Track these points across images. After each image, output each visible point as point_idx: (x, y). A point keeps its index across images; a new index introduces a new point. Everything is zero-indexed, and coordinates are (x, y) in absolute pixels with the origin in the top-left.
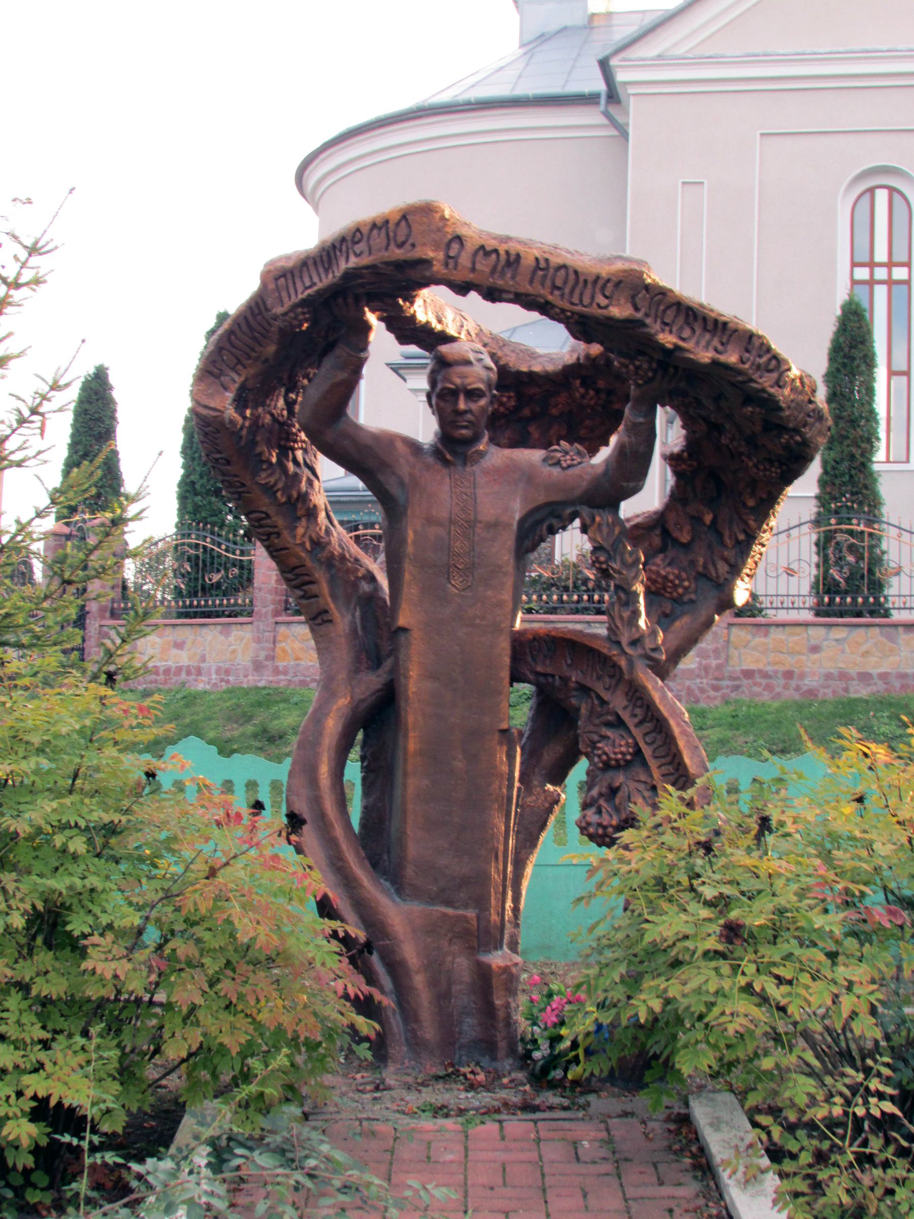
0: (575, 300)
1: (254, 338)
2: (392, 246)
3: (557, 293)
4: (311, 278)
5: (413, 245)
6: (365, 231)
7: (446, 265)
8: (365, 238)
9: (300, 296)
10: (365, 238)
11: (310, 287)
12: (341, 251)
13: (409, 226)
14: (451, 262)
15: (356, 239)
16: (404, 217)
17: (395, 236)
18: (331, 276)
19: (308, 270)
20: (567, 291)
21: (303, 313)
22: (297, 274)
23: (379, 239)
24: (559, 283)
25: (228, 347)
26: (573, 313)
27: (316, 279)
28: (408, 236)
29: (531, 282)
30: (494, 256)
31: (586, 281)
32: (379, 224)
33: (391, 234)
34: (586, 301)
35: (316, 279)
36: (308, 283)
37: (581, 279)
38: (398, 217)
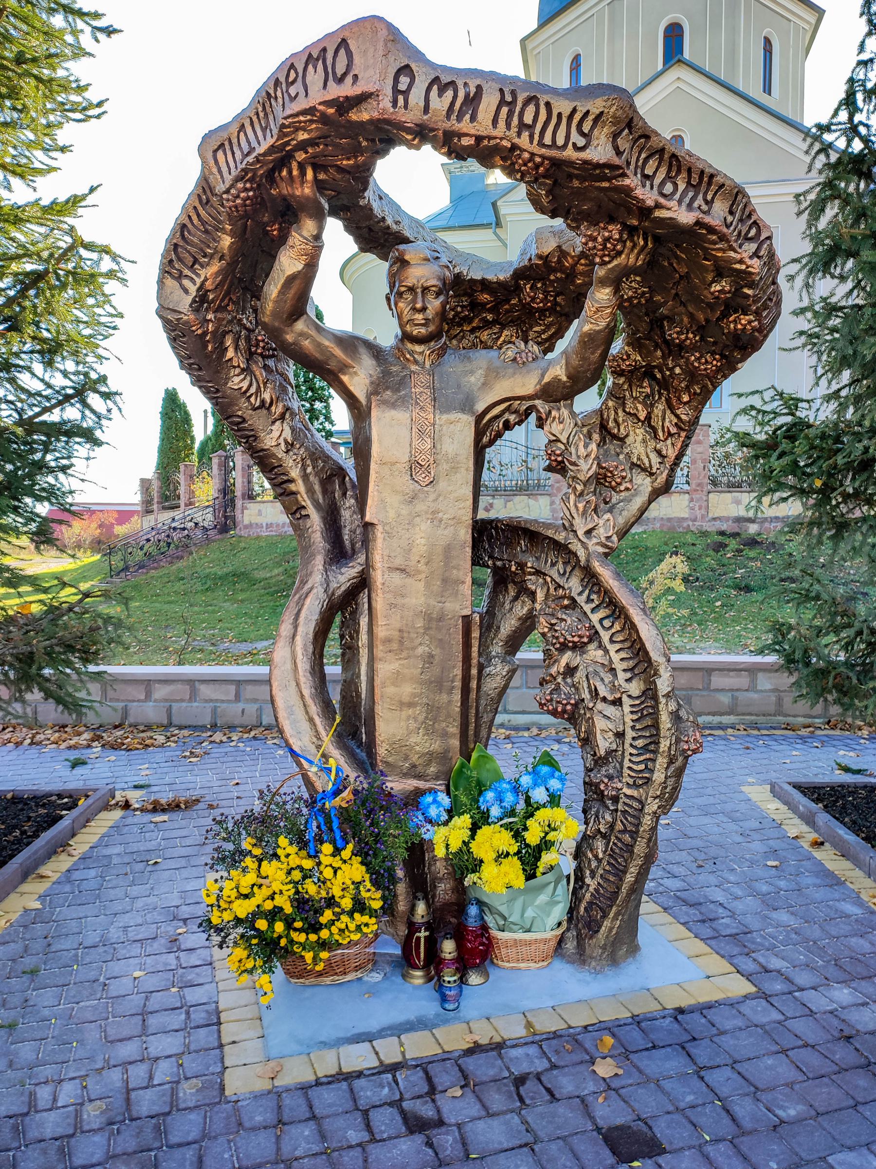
0: (548, 140)
1: (206, 232)
2: (331, 83)
7: (395, 103)
9: (240, 167)
10: (300, 75)
12: (276, 98)
13: (349, 55)
14: (401, 99)
15: (291, 80)
16: (344, 41)
19: (246, 134)
21: (246, 190)
22: (235, 141)
23: (315, 77)
25: (181, 243)
26: (543, 157)
28: (349, 67)
29: (495, 122)
30: (449, 93)
31: (560, 115)
34: (560, 141)
35: (254, 144)
36: (246, 150)
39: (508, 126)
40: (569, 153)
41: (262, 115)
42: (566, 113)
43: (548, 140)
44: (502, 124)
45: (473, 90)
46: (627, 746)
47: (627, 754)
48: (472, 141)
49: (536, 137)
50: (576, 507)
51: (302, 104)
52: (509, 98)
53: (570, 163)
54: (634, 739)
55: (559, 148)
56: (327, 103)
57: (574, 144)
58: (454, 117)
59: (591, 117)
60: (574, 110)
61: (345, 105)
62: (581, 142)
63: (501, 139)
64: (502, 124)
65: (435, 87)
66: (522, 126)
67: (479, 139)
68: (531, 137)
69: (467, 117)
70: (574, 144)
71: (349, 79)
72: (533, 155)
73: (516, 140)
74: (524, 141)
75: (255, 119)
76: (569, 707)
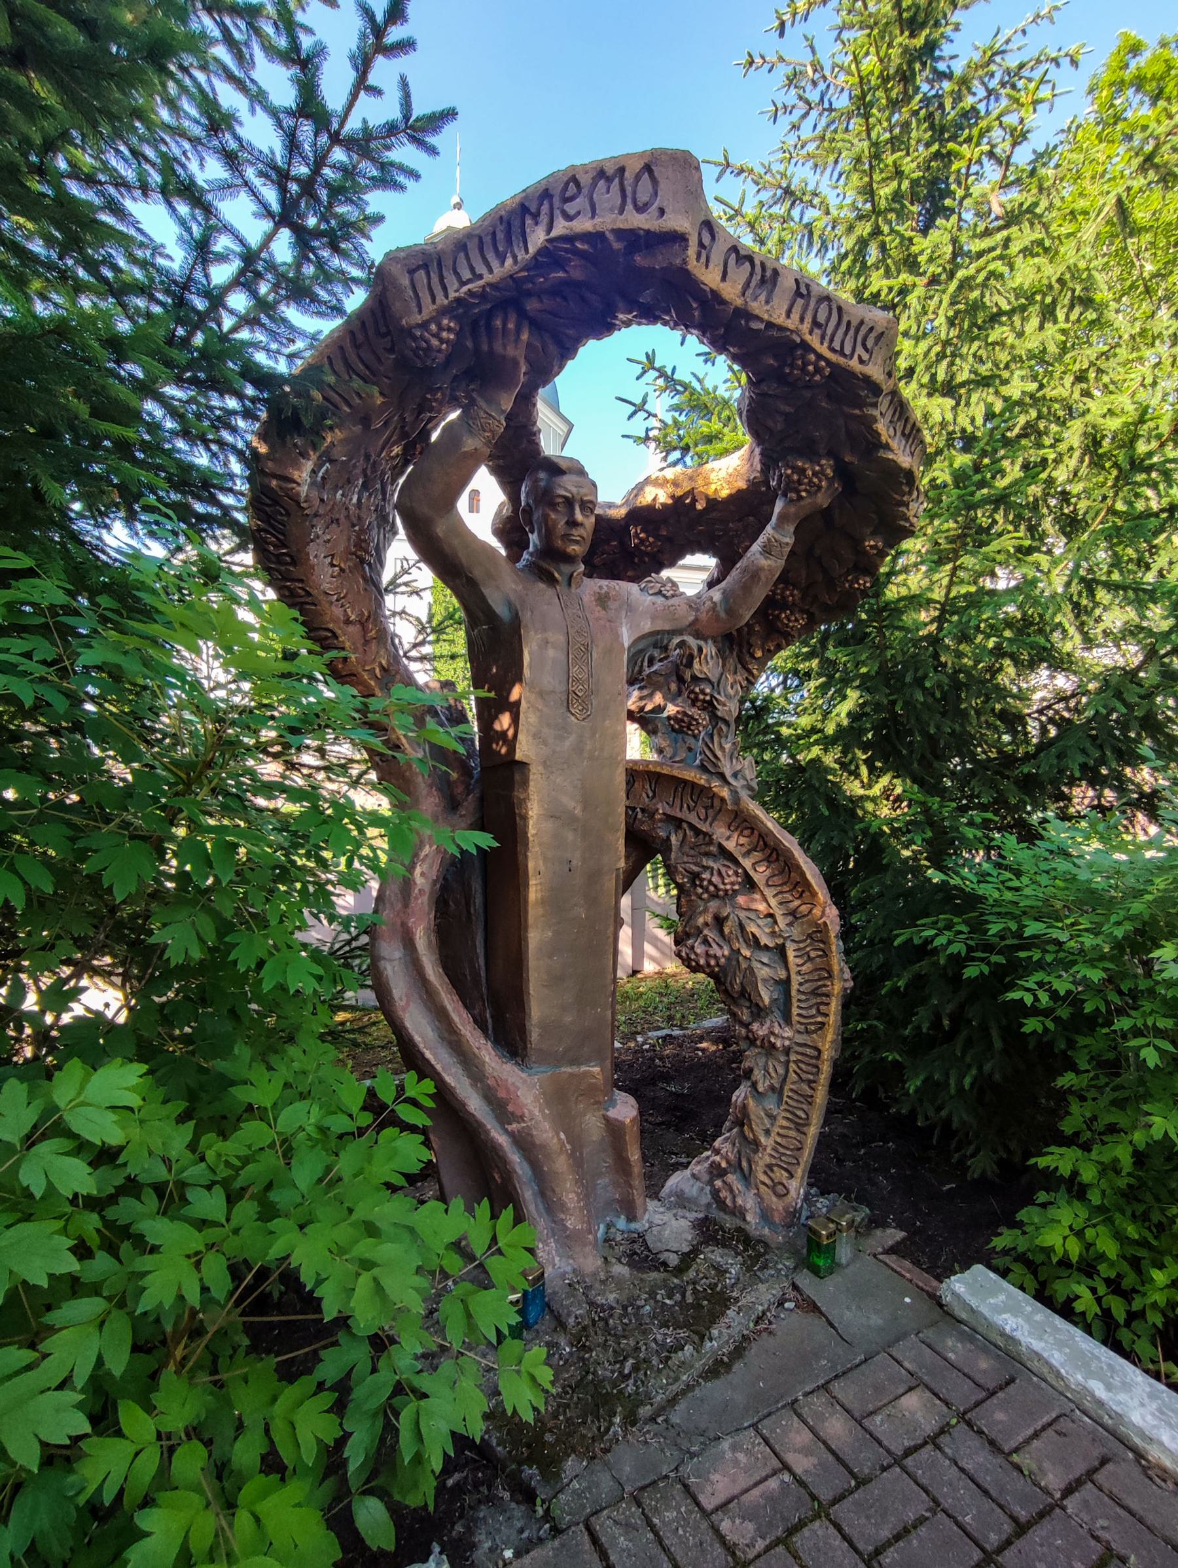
2: (629, 206)
3: (817, 331)
4: (472, 269)
5: (662, 212)
6: (585, 180)
8: (585, 191)
9: (452, 295)
11: (469, 281)
12: (536, 216)
13: (654, 181)
14: (704, 253)
15: (568, 194)
16: (648, 168)
17: (634, 192)
18: (509, 262)
20: (829, 331)
24: (821, 318)
27: (481, 269)
29: (788, 314)
31: (849, 323)
32: (610, 171)
33: (629, 190)
34: (847, 351)
35: (481, 269)
37: (845, 319)
38: (639, 165)
39: (802, 320)
40: (854, 364)
41: (500, 236)
42: (854, 323)
43: (837, 345)
44: (796, 316)
45: (768, 273)
46: (794, 993)
47: (794, 1001)
48: (762, 326)
49: (827, 338)
50: (722, 748)
51: (583, 225)
52: (803, 290)
53: (852, 374)
54: (801, 984)
55: (845, 356)
56: (619, 233)
57: (860, 357)
58: (749, 292)
59: (873, 335)
60: (862, 323)
61: (637, 240)
62: (865, 357)
63: (792, 331)
64: (796, 316)
65: (733, 255)
66: (816, 324)
67: (770, 325)
68: (823, 338)
69: (762, 298)
70: (860, 357)
71: (653, 208)
72: (820, 357)
73: (808, 337)
74: (814, 341)
75: (487, 240)
76: (723, 960)
